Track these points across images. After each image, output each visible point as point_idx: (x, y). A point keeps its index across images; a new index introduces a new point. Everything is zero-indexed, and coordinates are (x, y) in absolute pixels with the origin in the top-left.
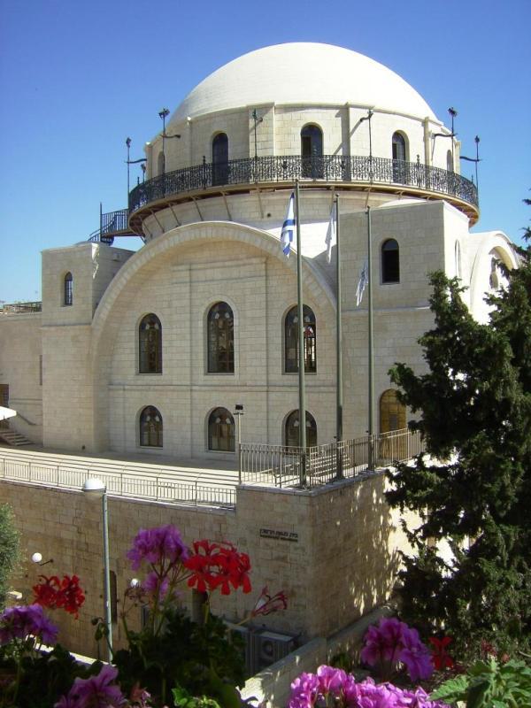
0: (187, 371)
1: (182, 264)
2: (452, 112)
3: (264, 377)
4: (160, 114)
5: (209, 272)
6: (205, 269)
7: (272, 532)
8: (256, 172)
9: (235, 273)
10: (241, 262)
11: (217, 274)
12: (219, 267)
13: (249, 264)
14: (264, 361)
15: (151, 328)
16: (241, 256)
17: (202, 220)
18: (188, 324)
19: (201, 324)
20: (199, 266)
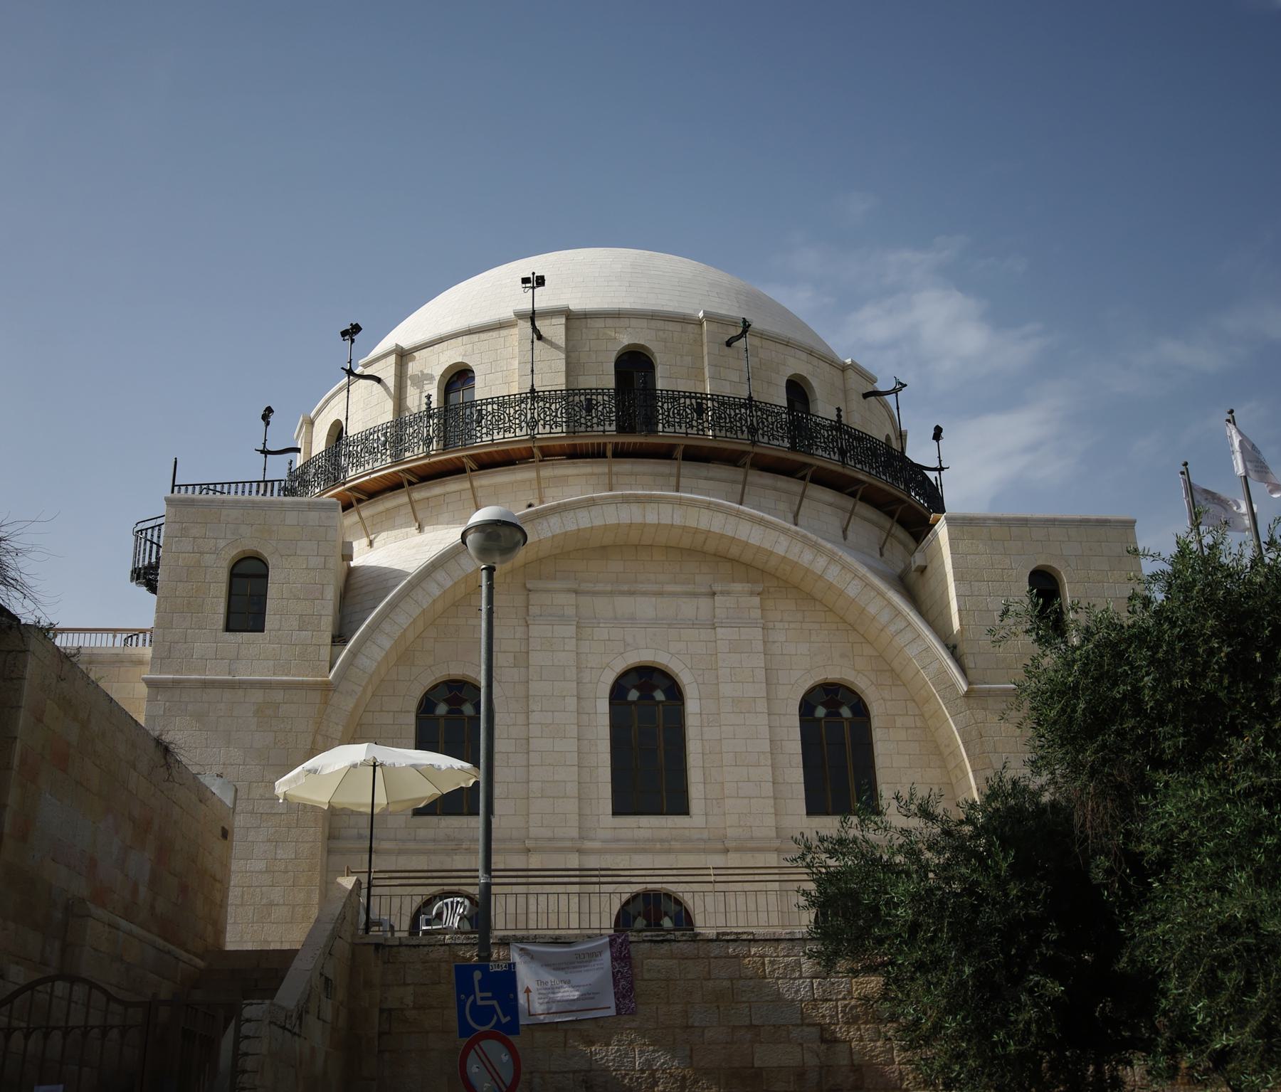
0: (572, 806)
3: (770, 821)
4: (525, 281)
5: (624, 605)
6: (612, 593)
8: (752, 424)
9: (688, 608)
11: (645, 607)
12: (644, 594)
13: (722, 593)
14: (768, 789)
15: (449, 712)
17: (611, 490)
18: (572, 703)
19: (604, 706)
20: (600, 587)
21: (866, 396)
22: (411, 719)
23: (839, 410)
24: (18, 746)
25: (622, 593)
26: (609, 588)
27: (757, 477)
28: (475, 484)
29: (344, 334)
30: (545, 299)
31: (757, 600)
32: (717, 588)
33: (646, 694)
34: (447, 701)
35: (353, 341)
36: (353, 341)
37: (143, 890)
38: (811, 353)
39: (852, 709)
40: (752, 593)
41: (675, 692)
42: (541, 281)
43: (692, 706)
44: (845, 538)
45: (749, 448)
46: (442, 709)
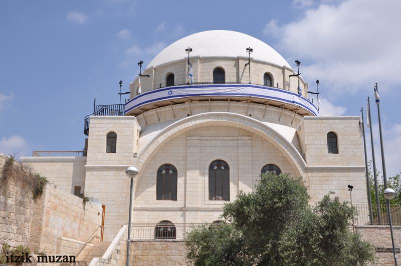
1: (194, 136)
2: (318, 82)
4: (187, 50)
6: (210, 140)
7: (382, 249)
10: (234, 138)
11: (219, 143)
12: (219, 140)
15: (166, 173)
16: (234, 135)
20: (206, 138)
21: (290, 76)
22: (155, 175)
23: (278, 84)
24: (45, 208)
25: (213, 140)
26: (209, 138)
27: (251, 106)
28: (174, 108)
29: (139, 64)
30: (192, 54)
31: (250, 141)
32: (239, 138)
33: (219, 168)
34: (165, 170)
35: (141, 67)
36: (141, 67)
37: (76, 231)
38: (273, 65)
39: (276, 171)
40: (249, 139)
41: (227, 167)
42: (191, 50)
43: (231, 171)
44: (279, 120)
45: (249, 98)
46: (164, 172)
